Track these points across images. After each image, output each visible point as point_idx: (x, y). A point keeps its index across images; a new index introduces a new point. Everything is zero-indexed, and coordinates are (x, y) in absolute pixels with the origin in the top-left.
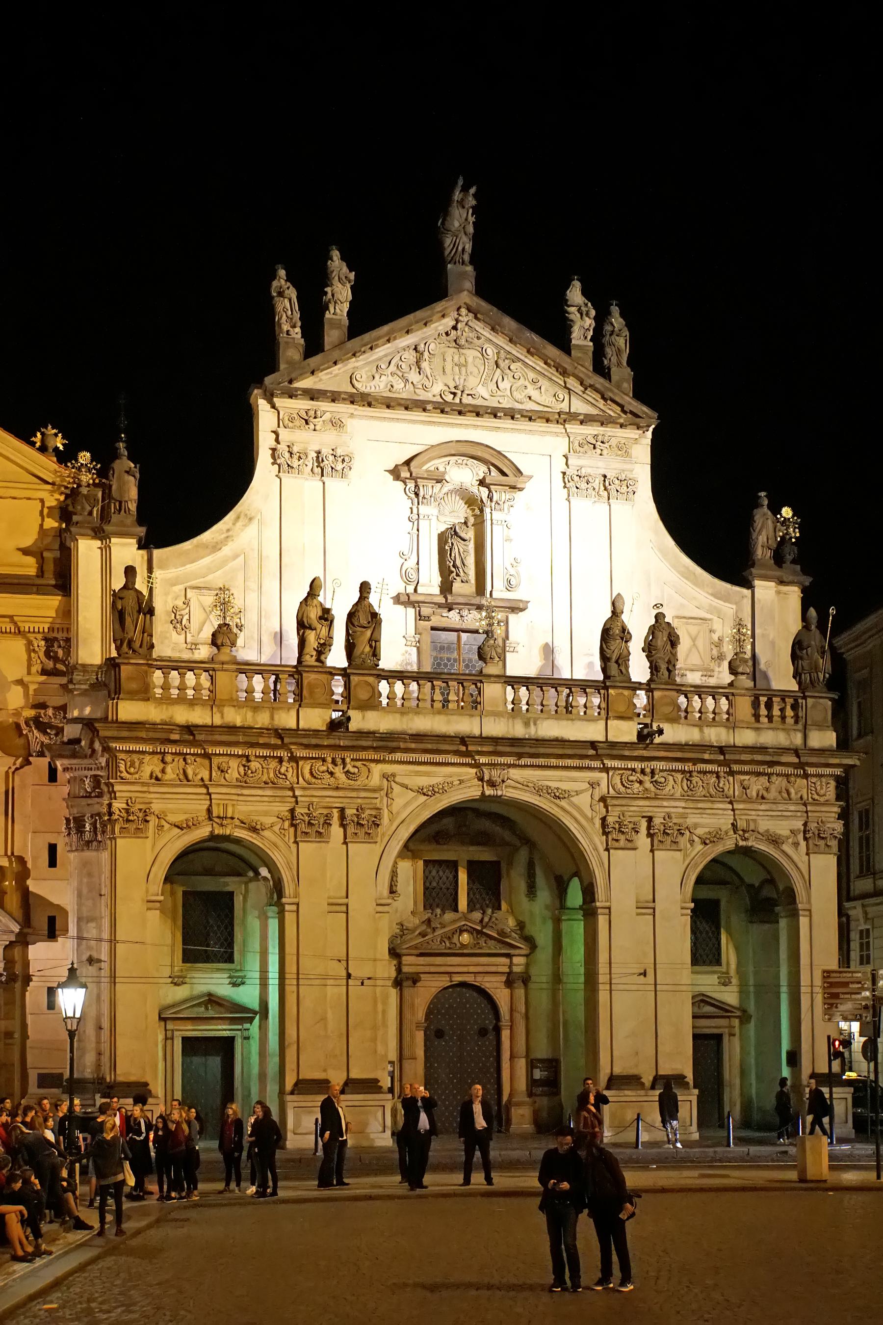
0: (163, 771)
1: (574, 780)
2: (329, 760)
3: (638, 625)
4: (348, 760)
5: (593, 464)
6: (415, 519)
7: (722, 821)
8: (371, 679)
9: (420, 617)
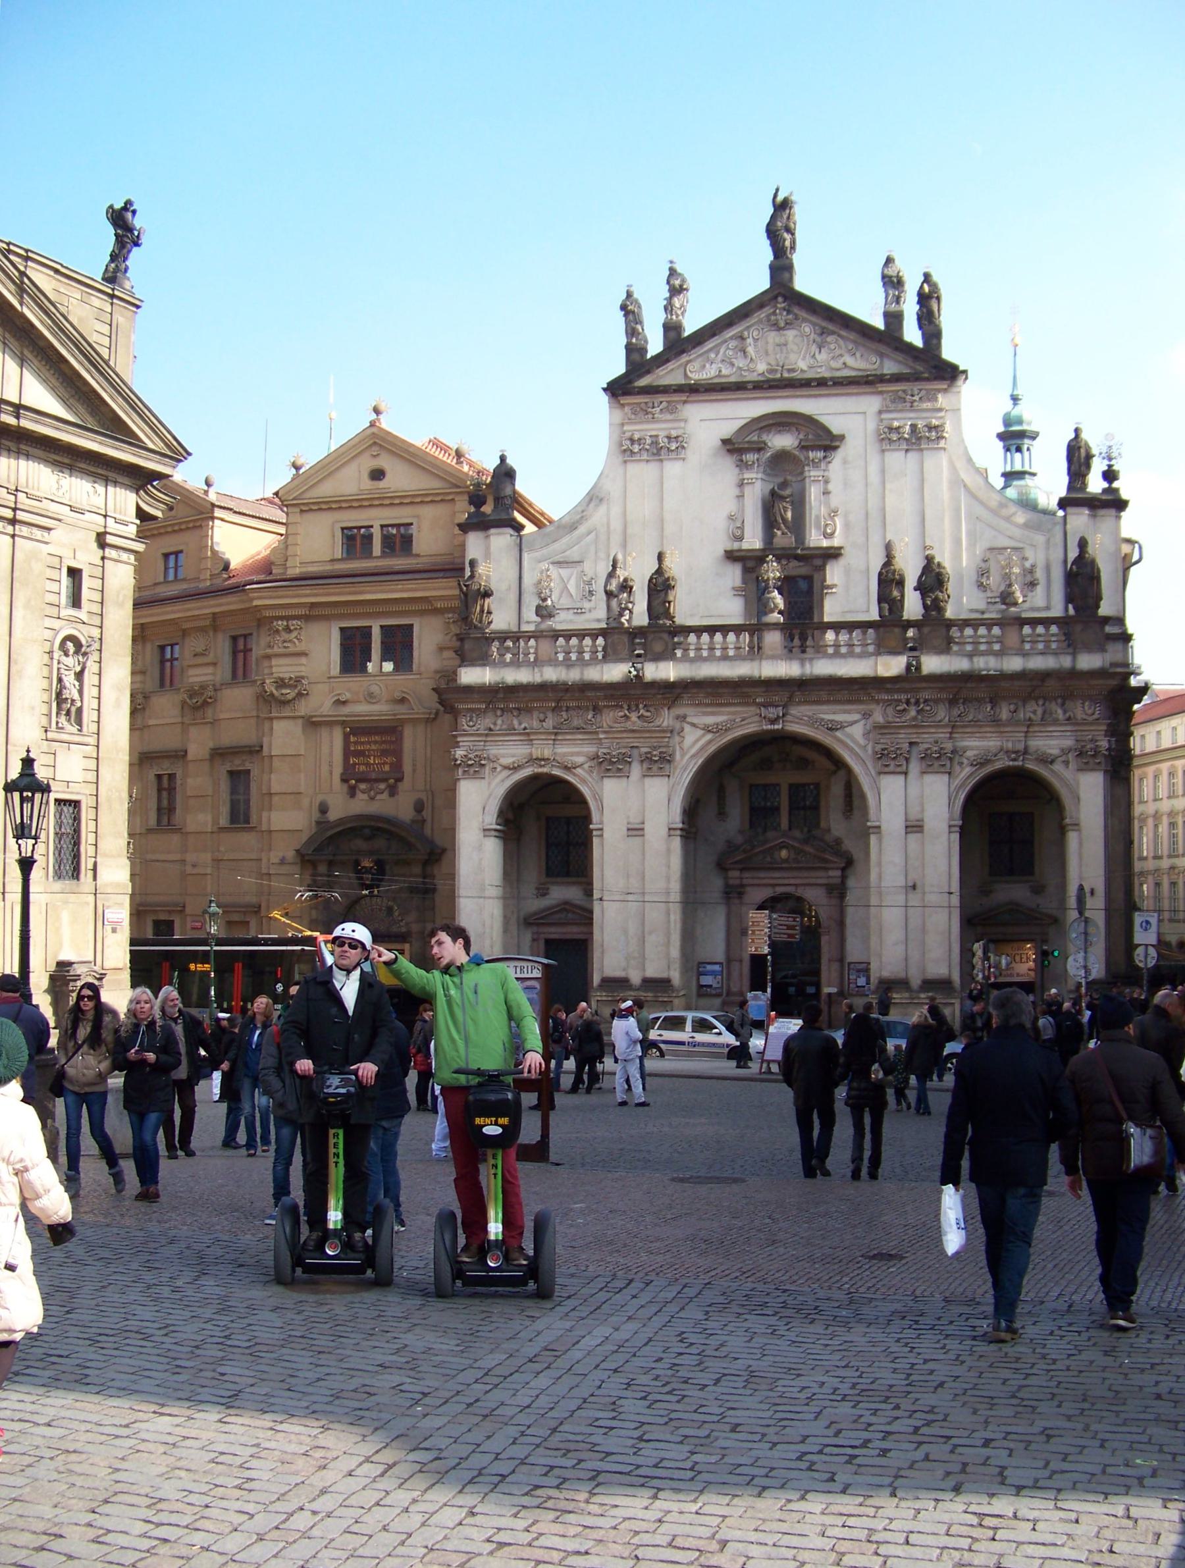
0: (495, 724)
1: (849, 712)
2: (626, 707)
3: (910, 568)
4: (641, 706)
5: (903, 421)
6: (741, 484)
7: (992, 743)
8: (665, 636)
9: (746, 571)
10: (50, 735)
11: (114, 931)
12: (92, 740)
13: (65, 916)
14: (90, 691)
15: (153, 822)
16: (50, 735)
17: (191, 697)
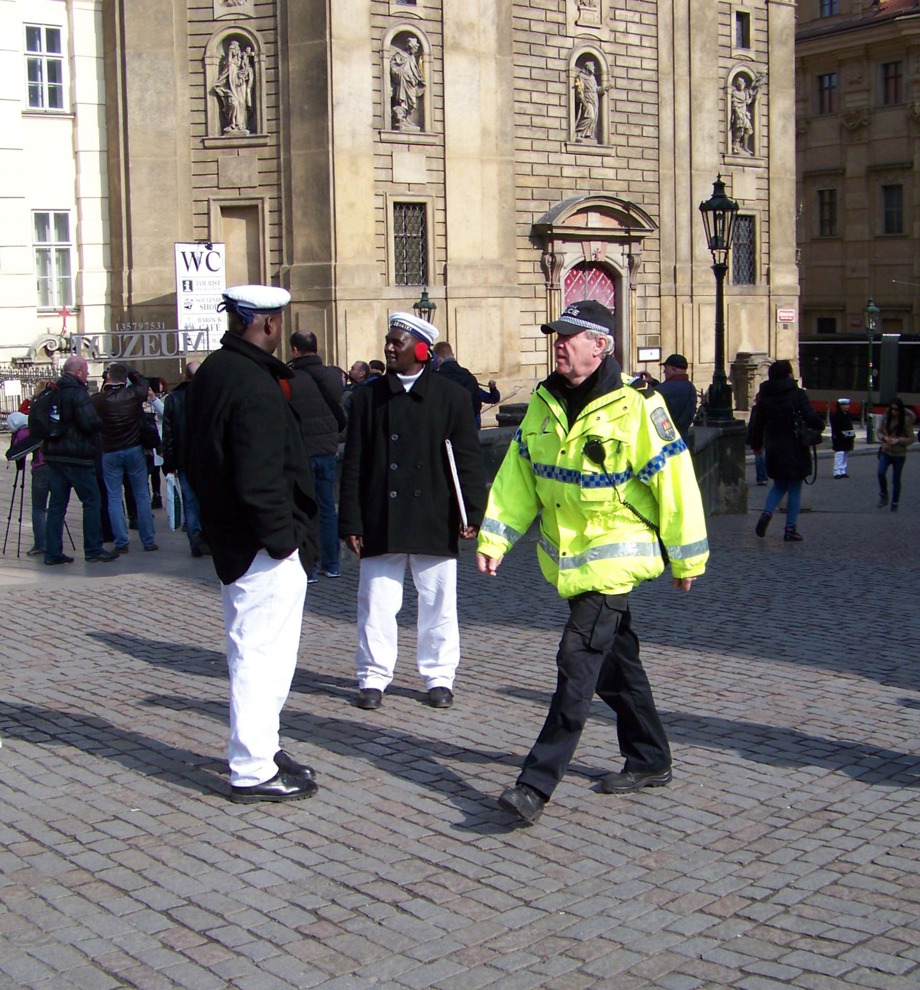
10: (727, 160)
11: (785, 327)
12: (763, 163)
13: (744, 315)
14: (760, 121)
15: (816, 232)
16: (727, 160)
17: (848, 121)
